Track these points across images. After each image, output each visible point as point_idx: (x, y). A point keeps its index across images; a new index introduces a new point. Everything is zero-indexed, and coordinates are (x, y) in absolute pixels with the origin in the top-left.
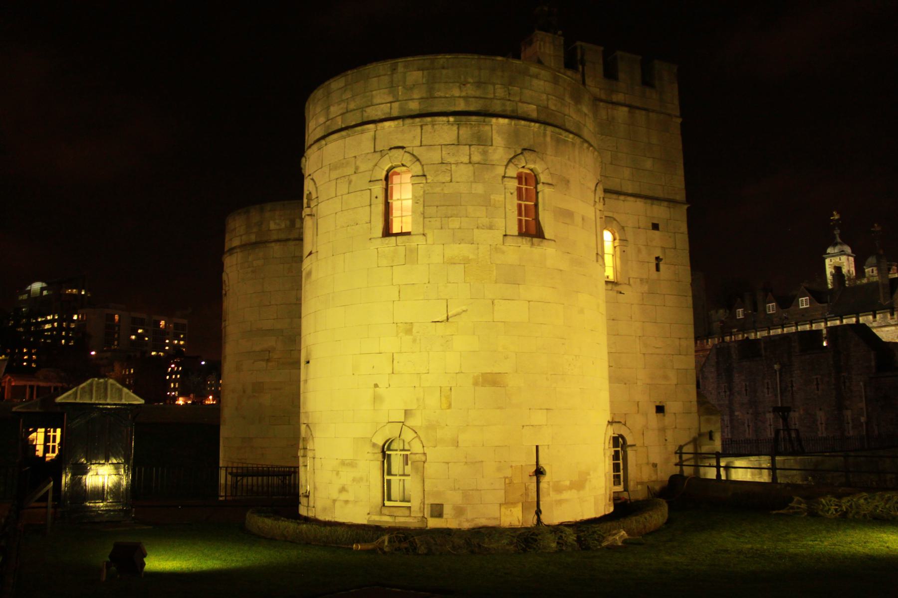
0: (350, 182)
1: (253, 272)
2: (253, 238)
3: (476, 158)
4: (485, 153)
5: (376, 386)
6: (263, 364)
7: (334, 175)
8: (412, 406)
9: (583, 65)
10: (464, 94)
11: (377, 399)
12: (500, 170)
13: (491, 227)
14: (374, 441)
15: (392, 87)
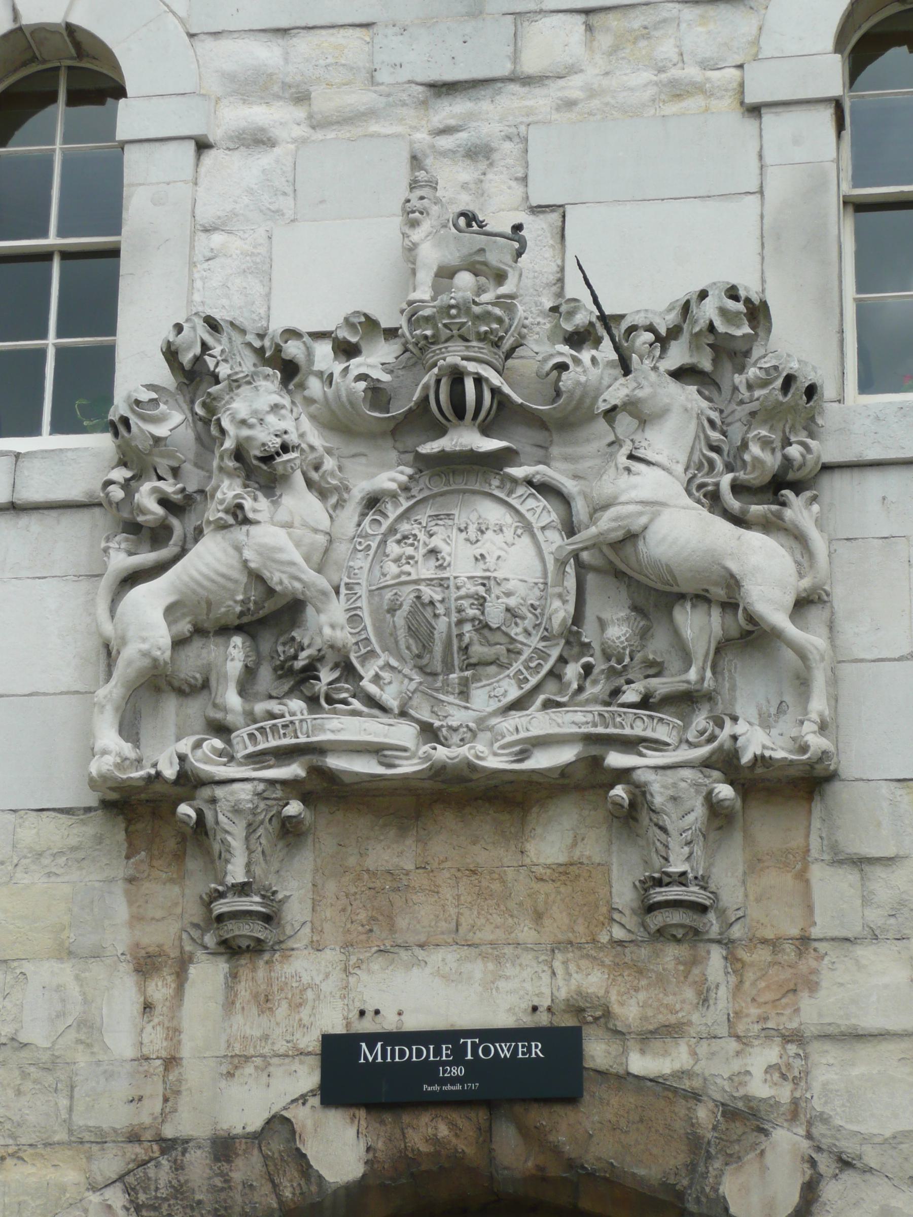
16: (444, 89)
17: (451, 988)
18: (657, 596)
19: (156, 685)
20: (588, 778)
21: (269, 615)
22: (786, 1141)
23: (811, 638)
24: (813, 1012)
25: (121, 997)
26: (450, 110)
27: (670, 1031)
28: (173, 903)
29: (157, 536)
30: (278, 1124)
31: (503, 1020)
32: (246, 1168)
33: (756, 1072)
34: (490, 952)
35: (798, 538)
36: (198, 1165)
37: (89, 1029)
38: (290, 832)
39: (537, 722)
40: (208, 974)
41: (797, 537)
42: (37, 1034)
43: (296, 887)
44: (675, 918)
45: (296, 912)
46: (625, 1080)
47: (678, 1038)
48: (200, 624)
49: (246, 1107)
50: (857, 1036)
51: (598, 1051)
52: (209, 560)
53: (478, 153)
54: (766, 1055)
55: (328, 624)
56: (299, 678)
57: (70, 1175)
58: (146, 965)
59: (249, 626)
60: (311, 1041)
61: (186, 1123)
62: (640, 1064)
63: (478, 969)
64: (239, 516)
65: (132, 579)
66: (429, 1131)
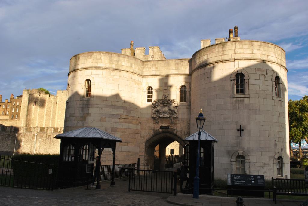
0: (265, 77)
1: (113, 80)
2: (114, 66)
5: (275, 141)
6: (117, 120)
7: (258, 72)
11: (276, 145)
14: (275, 157)
16: (165, 89)
17: (164, 125)
18: (172, 111)
19: (154, 113)
20: (169, 117)
21: (158, 111)
22: (176, 130)
23: (177, 113)
24: (177, 126)
25: (153, 125)
26: (165, 90)
27: (172, 127)
28: (155, 121)
29: (154, 108)
30: (159, 129)
31: (166, 126)
32: (157, 131)
33: (175, 128)
34: (166, 124)
35: (177, 109)
36: (156, 131)
37: (152, 126)
38: (159, 119)
39: (167, 115)
40: (156, 124)
41: (177, 109)
42: (150, 126)
43: (159, 121)
44: (172, 123)
45: (159, 122)
46: (170, 128)
47: (172, 127)
48: (155, 111)
49: (157, 129)
50: (178, 127)
51: (169, 127)
52: (156, 109)
53: (166, 92)
54: (175, 128)
55: (160, 112)
56: (159, 113)
57: (151, 131)
58: (154, 123)
59: (157, 111)
60: (159, 126)
61: (155, 129)
62: (171, 128)
63: (165, 124)
64: (157, 108)
65: (153, 109)
66: (164, 130)
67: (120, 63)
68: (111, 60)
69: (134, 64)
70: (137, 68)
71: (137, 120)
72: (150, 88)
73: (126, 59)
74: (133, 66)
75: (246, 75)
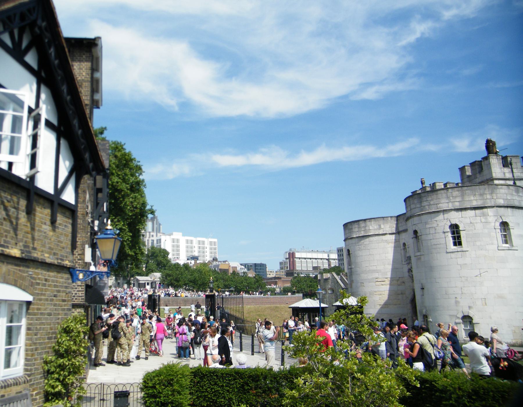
3: (483, 220)
4: (486, 219)
5: (456, 298)
8: (472, 305)
9: (511, 165)
10: (475, 198)
12: (493, 224)
13: (492, 244)
14: (458, 316)
15: (448, 198)
67: (367, 228)
68: (359, 228)
69: (383, 224)
70: (388, 226)
71: (398, 280)
72: (404, 244)
73: (372, 222)
74: (382, 226)
75: (419, 232)
